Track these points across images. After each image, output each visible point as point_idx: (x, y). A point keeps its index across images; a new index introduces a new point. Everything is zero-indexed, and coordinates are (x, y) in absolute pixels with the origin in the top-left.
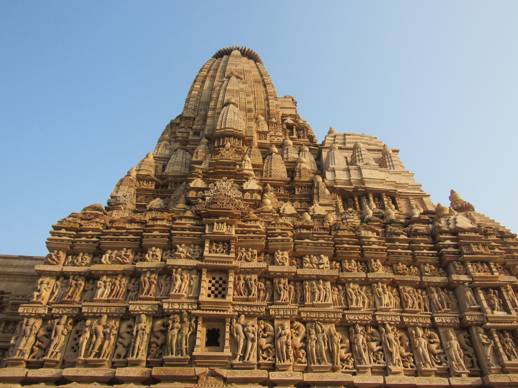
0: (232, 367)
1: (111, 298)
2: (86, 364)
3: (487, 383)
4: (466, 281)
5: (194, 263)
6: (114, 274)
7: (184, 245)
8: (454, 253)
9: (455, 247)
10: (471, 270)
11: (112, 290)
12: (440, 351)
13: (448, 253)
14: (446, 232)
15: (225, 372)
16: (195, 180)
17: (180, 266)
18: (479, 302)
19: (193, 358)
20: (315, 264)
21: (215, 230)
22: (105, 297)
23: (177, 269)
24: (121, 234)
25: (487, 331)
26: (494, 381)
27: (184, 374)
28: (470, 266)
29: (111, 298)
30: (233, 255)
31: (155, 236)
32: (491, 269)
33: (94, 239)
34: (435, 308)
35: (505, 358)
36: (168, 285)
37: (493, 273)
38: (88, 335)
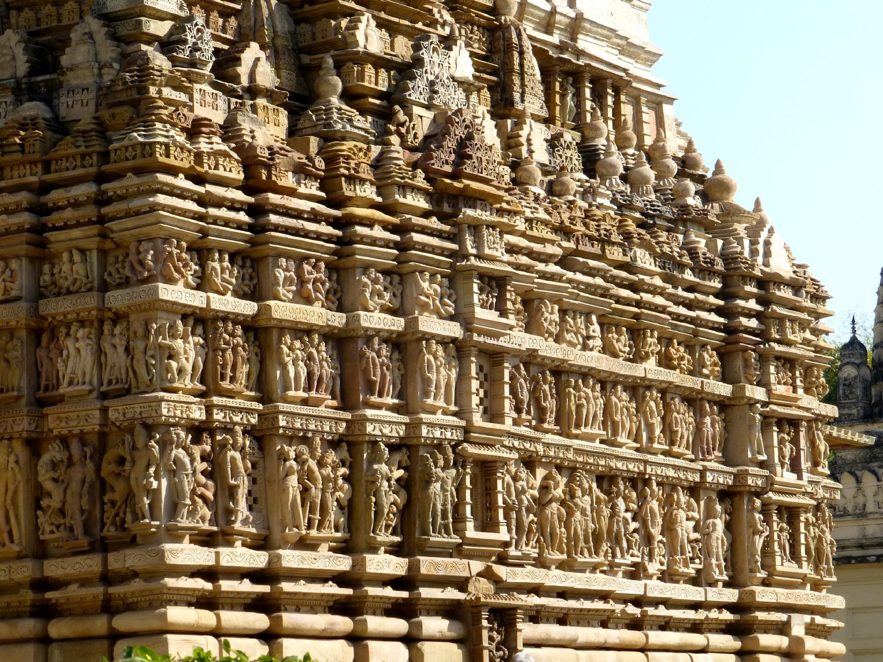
0: (502, 560)
1: (313, 394)
2: (303, 544)
3: (747, 600)
4: (758, 401)
5: (454, 330)
6: (303, 331)
7: (427, 274)
8: (752, 332)
9: (758, 315)
10: (773, 379)
11: (310, 375)
12: (697, 536)
13: (748, 330)
14: (752, 278)
15: (501, 571)
16: (364, 19)
17: (434, 336)
18: (769, 449)
19: (466, 541)
20: (582, 335)
21: (487, 251)
22: (302, 394)
23: (427, 340)
24: (298, 214)
25: (765, 510)
26: (760, 600)
27: (457, 574)
28: (772, 369)
29: (313, 394)
30: (512, 320)
31: (374, 242)
32: (794, 378)
33: (243, 217)
34: (702, 448)
35: (778, 560)
36: (396, 371)
37: (795, 391)
38: (293, 481)
